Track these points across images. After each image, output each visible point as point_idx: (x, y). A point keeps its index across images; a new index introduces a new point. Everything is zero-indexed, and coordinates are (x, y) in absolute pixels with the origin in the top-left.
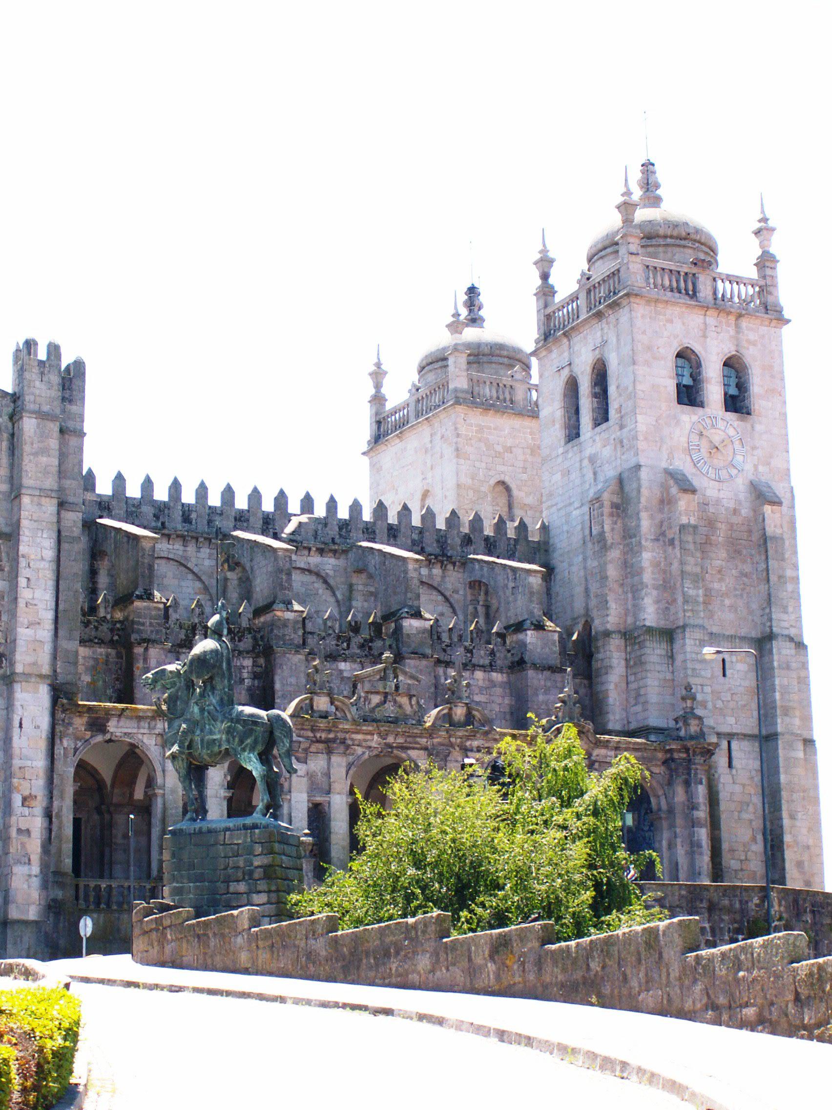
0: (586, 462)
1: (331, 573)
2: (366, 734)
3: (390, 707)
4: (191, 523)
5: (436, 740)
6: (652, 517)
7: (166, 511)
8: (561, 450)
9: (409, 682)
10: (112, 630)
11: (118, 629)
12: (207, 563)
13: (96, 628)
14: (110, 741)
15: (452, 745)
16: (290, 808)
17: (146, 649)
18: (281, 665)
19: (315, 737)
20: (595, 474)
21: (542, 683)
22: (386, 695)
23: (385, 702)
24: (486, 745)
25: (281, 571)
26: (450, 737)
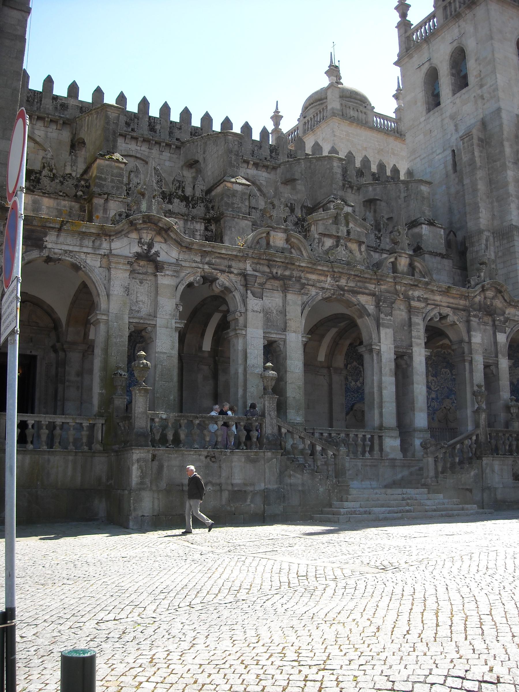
0: (447, 120)
1: (264, 183)
2: (320, 275)
3: (341, 253)
4: (155, 132)
5: (383, 287)
6: (511, 146)
7: (136, 120)
8: (423, 118)
9: (358, 229)
10: (76, 186)
11: (83, 186)
12: (167, 164)
13: (62, 183)
14: (48, 260)
15: (396, 293)
16: (245, 344)
17: (107, 200)
18: (230, 227)
19: (271, 273)
20: (456, 126)
21: (435, 265)
22: (338, 238)
23: (337, 246)
24: (425, 296)
25: (230, 151)
26: (396, 283)
